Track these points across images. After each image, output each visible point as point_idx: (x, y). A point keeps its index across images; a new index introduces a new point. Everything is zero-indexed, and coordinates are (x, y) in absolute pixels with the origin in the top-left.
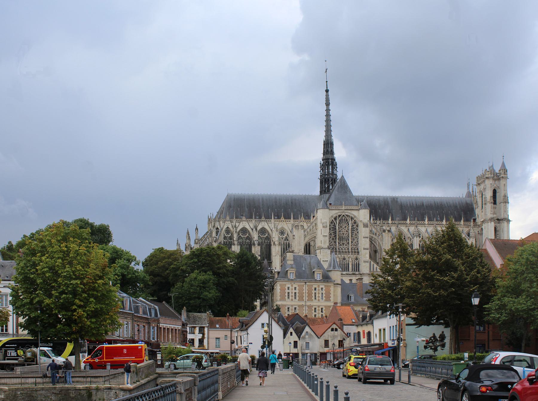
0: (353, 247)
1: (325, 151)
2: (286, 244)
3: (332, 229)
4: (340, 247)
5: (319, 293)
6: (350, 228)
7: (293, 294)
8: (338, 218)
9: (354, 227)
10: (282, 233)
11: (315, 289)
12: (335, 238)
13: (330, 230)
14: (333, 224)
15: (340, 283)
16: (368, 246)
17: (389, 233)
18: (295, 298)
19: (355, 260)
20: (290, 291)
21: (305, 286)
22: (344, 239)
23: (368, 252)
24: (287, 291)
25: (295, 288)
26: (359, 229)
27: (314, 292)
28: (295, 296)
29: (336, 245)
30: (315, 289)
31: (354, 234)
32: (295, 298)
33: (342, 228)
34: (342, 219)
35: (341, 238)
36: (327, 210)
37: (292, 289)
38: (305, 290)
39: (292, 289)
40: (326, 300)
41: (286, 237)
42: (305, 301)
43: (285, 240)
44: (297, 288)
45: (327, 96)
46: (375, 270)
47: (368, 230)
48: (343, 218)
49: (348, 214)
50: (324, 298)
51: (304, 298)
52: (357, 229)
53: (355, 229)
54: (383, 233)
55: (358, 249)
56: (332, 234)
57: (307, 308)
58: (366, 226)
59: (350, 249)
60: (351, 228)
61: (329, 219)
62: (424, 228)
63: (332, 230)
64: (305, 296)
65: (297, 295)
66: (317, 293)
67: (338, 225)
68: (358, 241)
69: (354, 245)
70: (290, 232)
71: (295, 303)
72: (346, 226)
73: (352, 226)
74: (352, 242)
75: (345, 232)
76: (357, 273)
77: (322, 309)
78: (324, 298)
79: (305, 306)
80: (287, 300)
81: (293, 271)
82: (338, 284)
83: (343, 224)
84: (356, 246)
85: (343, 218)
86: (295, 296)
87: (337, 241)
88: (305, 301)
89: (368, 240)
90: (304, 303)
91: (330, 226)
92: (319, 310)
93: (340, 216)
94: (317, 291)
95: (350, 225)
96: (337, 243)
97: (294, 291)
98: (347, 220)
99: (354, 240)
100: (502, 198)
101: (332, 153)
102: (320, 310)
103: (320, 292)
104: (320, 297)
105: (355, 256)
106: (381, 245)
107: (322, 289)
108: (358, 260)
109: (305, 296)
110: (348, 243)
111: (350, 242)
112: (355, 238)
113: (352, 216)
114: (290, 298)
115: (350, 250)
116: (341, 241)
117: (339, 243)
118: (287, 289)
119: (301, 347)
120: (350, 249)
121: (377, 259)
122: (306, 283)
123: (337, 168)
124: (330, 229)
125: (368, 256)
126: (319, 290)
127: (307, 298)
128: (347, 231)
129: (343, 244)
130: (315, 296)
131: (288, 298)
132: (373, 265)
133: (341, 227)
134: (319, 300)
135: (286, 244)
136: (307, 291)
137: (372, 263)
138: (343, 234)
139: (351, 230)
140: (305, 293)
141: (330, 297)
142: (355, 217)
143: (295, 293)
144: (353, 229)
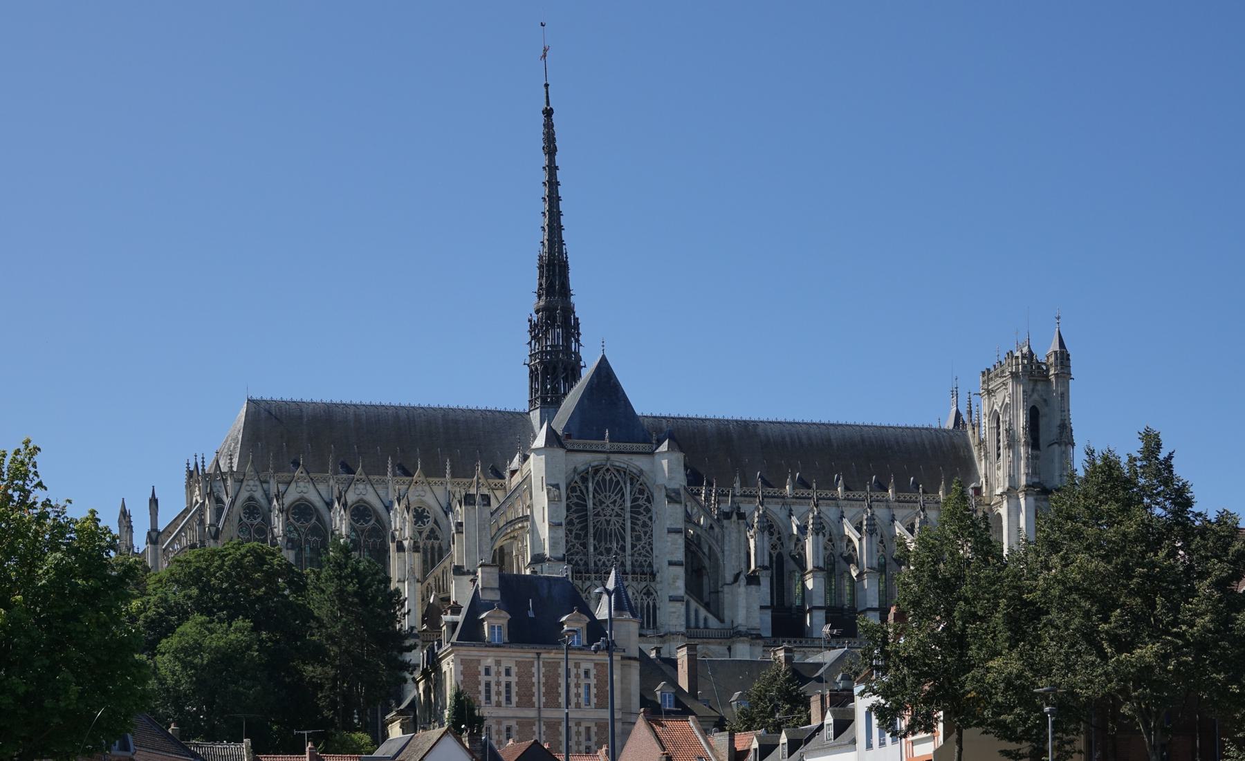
0: (636, 561)
1: (544, 286)
2: (433, 548)
3: (574, 508)
4: (600, 560)
5: (577, 686)
6: (628, 504)
7: (503, 689)
8: (593, 478)
9: (640, 502)
10: (420, 516)
12: (582, 533)
13: (568, 511)
14: (578, 493)
15: (637, 655)
16: (680, 555)
17: (741, 521)
18: (508, 699)
19: (644, 597)
20: (492, 679)
22: (611, 536)
23: (680, 571)
24: (483, 678)
25: (508, 673)
26: (653, 509)
28: (508, 692)
29: (586, 554)
31: (640, 523)
32: (508, 699)
33: (604, 506)
34: (604, 480)
35: (600, 535)
36: (561, 452)
37: (498, 673)
38: (536, 675)
39: (498, 673)
41: (432, 531)
42: (537, 705)
43: (428, 537)
44: (514, 670)
45: (549, 126)
46: (701, 624)
47: (678, 510)
48: (608, 478)
49: (622, 465)
51: (535, 699)
52: (648, 510)
53: (642, 510)
54: (725, 522)
55: (650, 565)
56: (576, 521)
57: (543, 728)
58: (673, 497)
59: (628, 563)
60: (631, 507)
61: (566, 477)
62: (834, 509)
63: (576, 512)
64: (536, 694)
65: (514, 689)
67: (591, 496)
68: (650, 544)
69: (640, 554)
70: (442, 514)
71: (509, 713)
72: (615, 501)
73: (634, 500)
74: (633, 546)
75: (614, 519)
76: (649, 632)
78: (594, 700)
79: (537, 723)
80: (483, 704)
81: (503, 619)
82: (630, 658)
83: (608, 494)
84: (645, 556)
85: (608, 478)
86: (508, 692)
87: (592, 540)
88: (537, 705)
89: (680, 540)
90: (531, 713)
91: (568, 498)
92: (578, 733)
93: (596, 471)
95: (628, 497)
96: (592, 549)
97: (503, 679)
98: (618, 482)
99: (638, 539)
100: (1055, 430)
101: (565, 292)
102: (583, 734)
104: (583, 695)
105: (644, 584)
106: (719, 555)
107: (587, 673)
108: (652, 597)
109: (536, 694)
110: (623, 549)
111: (628, 546)
112: (642, 535)
113: (635, 471)
114: (494, 698)
115: (628, 568)
116: (603, 543)
117: (595, 549)
118: (483, 672)
120: (628, 563)
121: (706, 593)
122: (539, 654)
123: (579, 334)
124: (568, 508)
125: (681, 584)
126: (577, 676)
127: (543, 699)
128: (618, 515)
129: (609, 551)
131: (488, 698)
132: (697, 611)
133: (602, 503)
134: (578, 706)
135: (433, 548)
136: (543, 680)
137: (693, 604)
138: (608, 522)
139: (631, 512)
140: (536, 684)
142: (641, 472)
143: (508, 685)
144: (635, 510)
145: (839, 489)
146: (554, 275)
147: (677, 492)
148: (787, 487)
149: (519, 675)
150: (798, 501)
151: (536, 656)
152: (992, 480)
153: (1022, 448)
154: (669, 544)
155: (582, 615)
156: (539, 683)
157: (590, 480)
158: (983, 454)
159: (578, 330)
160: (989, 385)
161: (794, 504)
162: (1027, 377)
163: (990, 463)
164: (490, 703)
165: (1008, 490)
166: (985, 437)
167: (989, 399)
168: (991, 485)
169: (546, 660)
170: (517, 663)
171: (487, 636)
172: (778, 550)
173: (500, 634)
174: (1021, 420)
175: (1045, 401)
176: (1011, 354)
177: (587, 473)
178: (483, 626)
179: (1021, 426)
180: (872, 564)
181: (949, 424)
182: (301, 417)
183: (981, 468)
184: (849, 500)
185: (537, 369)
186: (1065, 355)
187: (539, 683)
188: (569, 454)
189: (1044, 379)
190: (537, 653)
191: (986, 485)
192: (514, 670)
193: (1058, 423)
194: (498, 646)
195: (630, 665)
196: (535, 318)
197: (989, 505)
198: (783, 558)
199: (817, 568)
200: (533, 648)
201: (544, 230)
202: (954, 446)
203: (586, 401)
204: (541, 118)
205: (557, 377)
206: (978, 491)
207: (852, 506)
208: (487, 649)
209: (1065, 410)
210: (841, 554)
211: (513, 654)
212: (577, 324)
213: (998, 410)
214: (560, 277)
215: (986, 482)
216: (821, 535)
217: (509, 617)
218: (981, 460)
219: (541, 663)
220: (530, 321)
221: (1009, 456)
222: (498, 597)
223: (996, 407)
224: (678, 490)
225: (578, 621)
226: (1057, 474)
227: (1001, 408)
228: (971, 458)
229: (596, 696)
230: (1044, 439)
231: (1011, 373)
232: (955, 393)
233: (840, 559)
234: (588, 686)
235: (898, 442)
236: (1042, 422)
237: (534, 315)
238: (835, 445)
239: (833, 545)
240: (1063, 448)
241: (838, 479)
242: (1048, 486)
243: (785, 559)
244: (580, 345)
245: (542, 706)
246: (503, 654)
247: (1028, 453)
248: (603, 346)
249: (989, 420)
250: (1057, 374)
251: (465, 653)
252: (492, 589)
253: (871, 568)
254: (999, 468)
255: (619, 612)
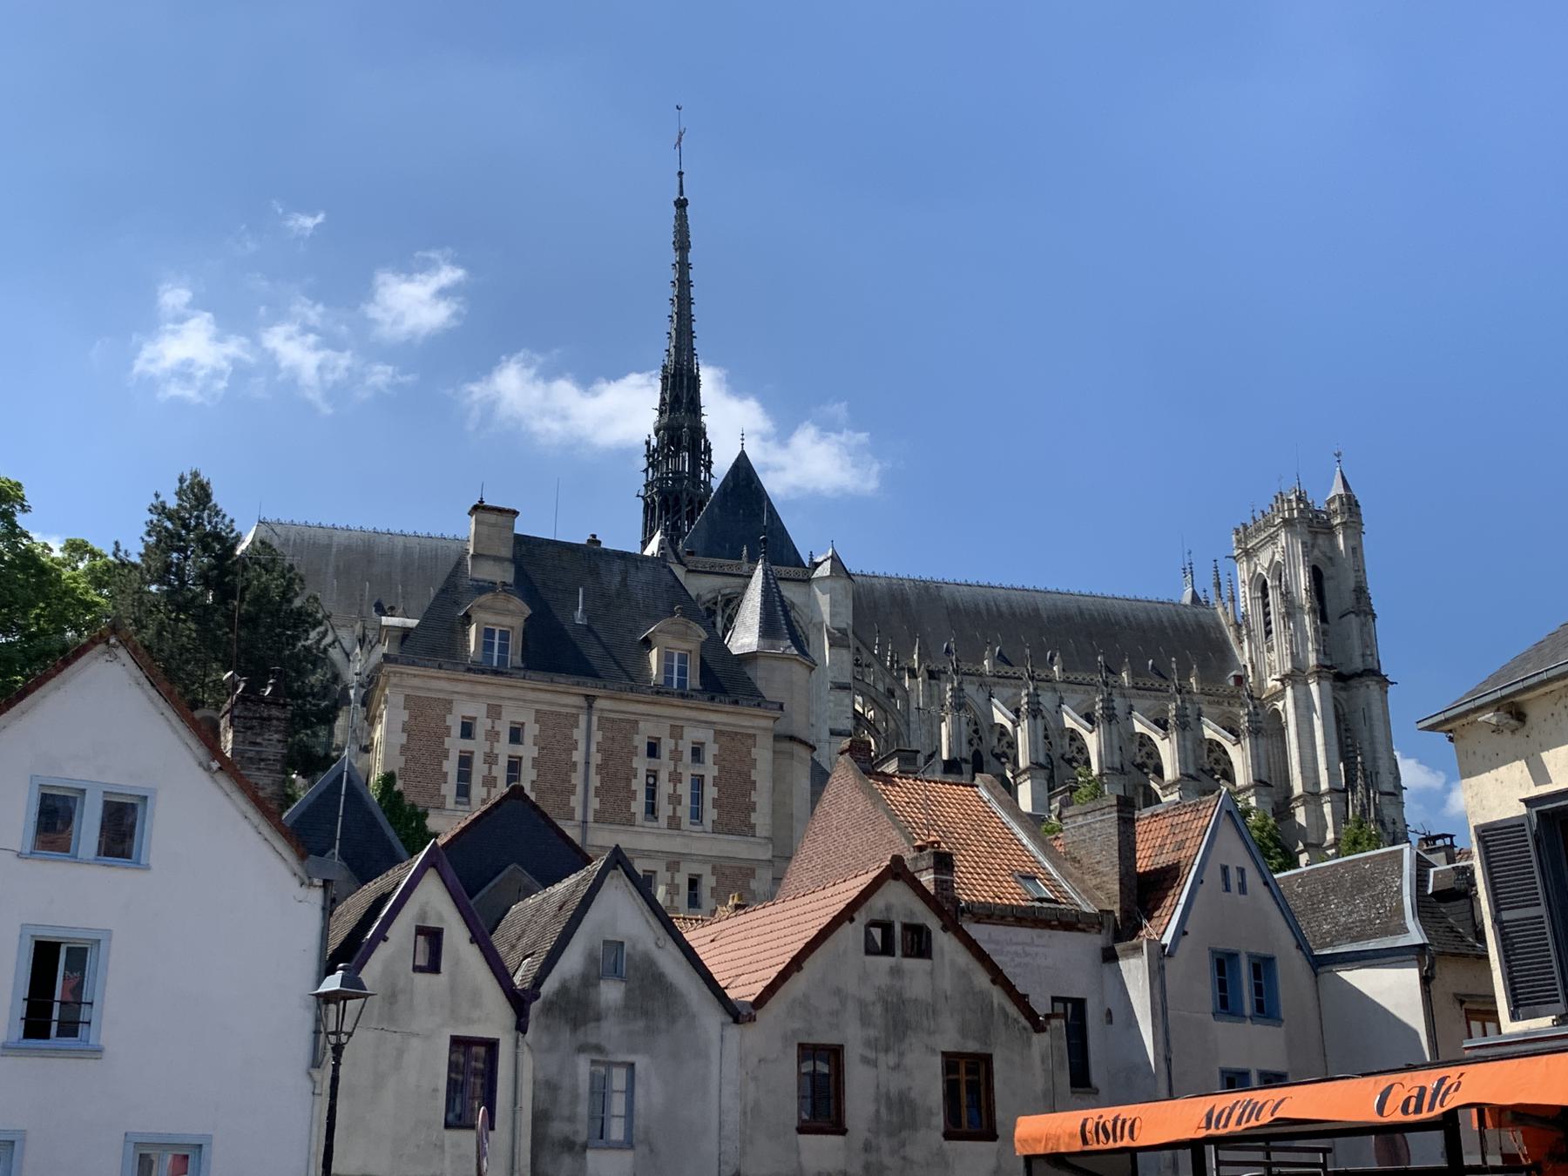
5: (675, 778)
11: (653, 750)
20: (478, 746)
21: (583, 719)
24: (455, 745)
25: (516, 735)
27: (641, 764)
30: (653, 750)
37: (493, 735)
38: (582, 746)
39: (493, 735)
40: (720, 828)
42: (578, 815)
44: (531, 730)
50: (710, 814)
66: (663, 776)
77: (693, 883)
80: (450, 801)
81: (511, 616)
88: (578, 815)
94: (664, 766)
97: (504, 749)
103: (688, 770)
104: (686, 800)
107: (697, 753)
109: (580, 789)
118: (456, 730)
119: (540, 1118)
122: (590, 699)
126: (676, 755)
127: (595, 803)
130: (651, 793)
134: (674, 823)
136: (596, 758)
140: (581, 768)
141: (752, 807)
145: (1055, 668)
146: (681, 388)
147: (843, 631)
148: (986, 662)
149: (543, 745)
150: (1001, 680)
151: (585, 704)
152: (1260, 667)
153: (1307, 618)
154: (832, 705)
155: (692, 624)
156: (587, 763)
157: (719, 612)
158: (1244, 632)
159: (710, 457)
160: (1246, 544)
161: (995, 684)
162: (1305, 525)
163: (1256, 648)
164: (469, 803)
165: (1292, 672)
166: (1247, 610)
167: (1248, 562)
168: (1260, 673)
169: (606, 715)
170: (540, 716)
171: (472, 648)
172: (975, 746)
173: (504, 648)
174: (1303, 580)
175: (1330, 559)
176: (1280, 498)
177: (715, 604)
178: (466, 634)
179: (1303, 587)
180: (1112, 763)
181: (1187, 598)
182: (329, 546)
183: (1244, 655)
184: (1069, 683)
185: (653, 500)
186: (1353, 502)
187: (587, 763)
188: (691, 575)
189: (1327, 531)
190: (587, 697)
191: (1253, 672)
192: (531, 730)
193: (1352, 585)
194: (496, 673)
195: (791, 755)
196: (654, 442)
197: (1259, 699)
198: (981, 757)
199: (1035, 766)
200: (578, 684)
201: (670, 338)
202: (1200, 626)
203: (716, 510)
204: (673, 210)
205: (679, 511)
206: (1240, 680)
207: (1074, 691)
208: (471, 676)
209: (1360, 570)
210: (1062, 757)
211: (531, 695)
212: (708, 450)
213: (1264, 573)
214: (688, 391)
215: (1253, 668)
216: (1039, 717)
217: (528, 611)
218: (1241, 642)
219: (595, 719)
220: (648, 443)
221: (1289, 628)
222: (509, 577)
223: (1259, 569)
224: (845, 629)
225: (683, 636)
226: (1357, 653)
227: (1268, 570)
228: (1226, 641)
229: (716, 803)
230: (1332, 608)
231: (1285, 520)
232: (1189, 570)
233: (1062, 761)
234: (698, 782)
235: (1126, 618)
236: (1328, 586)
237: (653, 436)
238: (1045, 616)
239: (1050, 743)
240: (1362, 617)
241: (1052, 659)
242: (1345, 670)
243: (985, 759)
244: (711, 476)
245: (591, 818)
246: (506, 692)
247: (1315, 622)
248: (743, 439)
249: (1250, 589)
250: (1345, 523)
251: (416, 682)
252: (497, 559)
253: (1112, 769)
254: (1270, 649)
255: (769, 642)
